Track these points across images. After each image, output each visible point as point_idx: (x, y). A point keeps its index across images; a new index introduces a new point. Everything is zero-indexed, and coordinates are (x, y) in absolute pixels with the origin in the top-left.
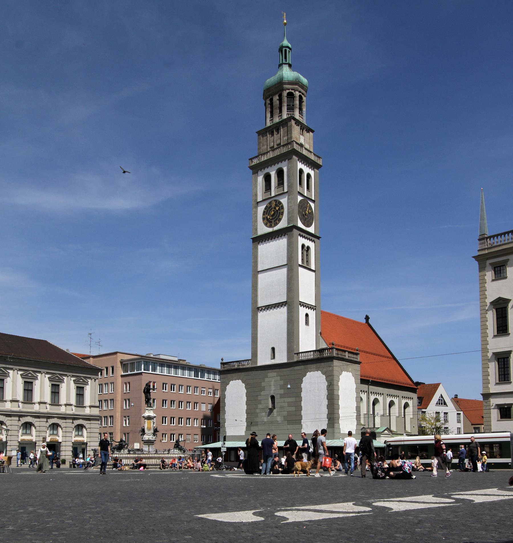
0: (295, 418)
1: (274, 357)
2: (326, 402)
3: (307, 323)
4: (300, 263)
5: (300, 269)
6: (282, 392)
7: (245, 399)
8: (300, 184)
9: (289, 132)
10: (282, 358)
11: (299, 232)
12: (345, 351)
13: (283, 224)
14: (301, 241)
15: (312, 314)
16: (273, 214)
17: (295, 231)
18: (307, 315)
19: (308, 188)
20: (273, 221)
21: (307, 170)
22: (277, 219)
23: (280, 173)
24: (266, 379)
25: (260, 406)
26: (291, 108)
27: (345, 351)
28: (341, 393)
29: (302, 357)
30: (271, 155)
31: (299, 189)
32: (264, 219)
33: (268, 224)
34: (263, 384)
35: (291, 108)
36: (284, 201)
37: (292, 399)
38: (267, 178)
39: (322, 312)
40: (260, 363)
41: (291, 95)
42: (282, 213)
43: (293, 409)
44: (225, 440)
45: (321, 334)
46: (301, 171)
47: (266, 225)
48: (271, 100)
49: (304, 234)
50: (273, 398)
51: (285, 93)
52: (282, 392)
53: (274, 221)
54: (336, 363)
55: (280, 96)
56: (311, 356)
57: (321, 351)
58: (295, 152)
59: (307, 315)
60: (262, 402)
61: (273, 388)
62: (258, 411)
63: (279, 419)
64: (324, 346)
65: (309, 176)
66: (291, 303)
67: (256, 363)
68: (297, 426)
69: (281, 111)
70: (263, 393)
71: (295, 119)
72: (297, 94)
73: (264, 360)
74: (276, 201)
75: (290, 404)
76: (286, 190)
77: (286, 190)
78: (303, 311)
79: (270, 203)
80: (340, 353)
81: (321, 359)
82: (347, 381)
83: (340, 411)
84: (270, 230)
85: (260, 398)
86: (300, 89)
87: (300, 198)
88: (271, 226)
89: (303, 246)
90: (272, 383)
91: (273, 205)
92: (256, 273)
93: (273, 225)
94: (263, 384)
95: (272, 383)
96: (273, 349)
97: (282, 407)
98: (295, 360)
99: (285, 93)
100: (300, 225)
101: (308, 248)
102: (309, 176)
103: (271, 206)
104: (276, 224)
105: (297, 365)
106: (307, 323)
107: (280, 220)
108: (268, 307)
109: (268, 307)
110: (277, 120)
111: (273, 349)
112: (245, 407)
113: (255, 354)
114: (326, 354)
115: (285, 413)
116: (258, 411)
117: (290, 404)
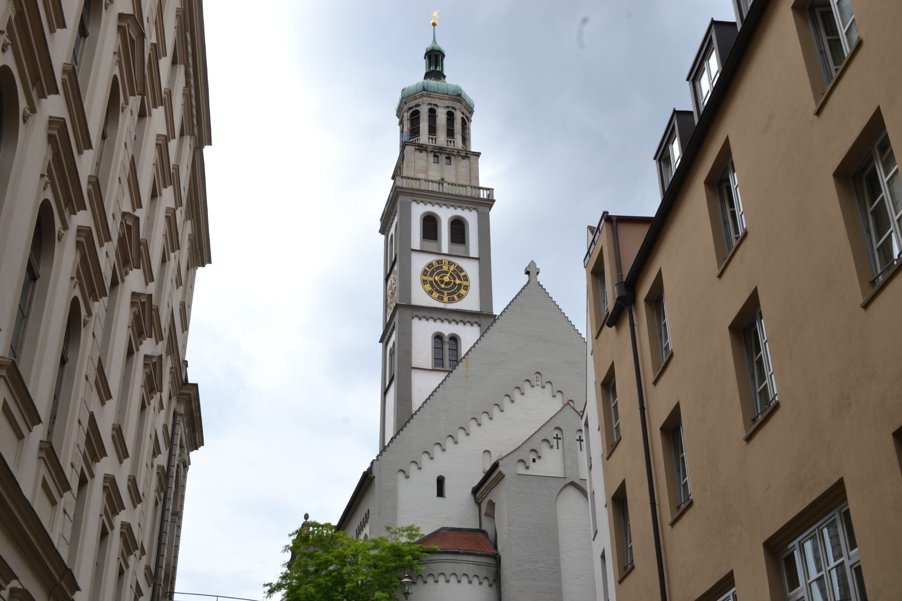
13: (470, 302)
20: (446, 292)
22: (454, 293)
32: (424, 282)
36: (471, 269)
42: (466, 288)
47: (430, 293)
53: (448, 294)
76: (474, 251)
79: (439, 262)
88: (440, 299)
91: (445, 268)
93: (446, 299)
103: (441, 267)
104: (452, 300)
107: (461, 297)
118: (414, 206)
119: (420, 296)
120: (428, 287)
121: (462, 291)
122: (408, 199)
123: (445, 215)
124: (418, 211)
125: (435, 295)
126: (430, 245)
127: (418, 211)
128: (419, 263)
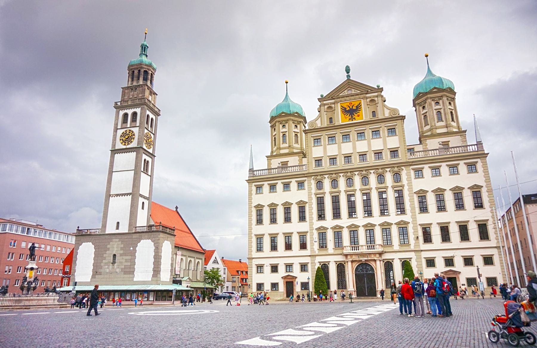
0: (130, 270)
1: (118, 228)
2: (153, 260)
3: (143, 208)
4: (142, 170)
5: (142, 173)
6: (122, 252)
7: (93, 256)
8: (147, 123)
9: (143, 92)
10: (124, 229)
11: (144, 151)
12: (167, 228)
14: (144, 157)
15: (146, 202)
16: (127, 138)
17: (141, 149)
18: (143, 203)
19: (151, 126)
21: (151, 116)
23: (135, 114)
24: (111, 243)
25: (104, 261)
26: (145, 79)
27: (167, 228)
28: (162, 254)
29: (138, 230)
30: (130, 103)
31: (146, 126)
32: (120, 140)
33: (123, 143)
34: (108, 246)
35: (145, 79)
36: (136, 130)
37: (129, 257)
38: (126, 115)
39: (153, 202)
40: (107, 233)
41: (146, 72)
43: (129, 264)
44: (75, 284)
45: (150, 216)
46: (148, 116)
48: (133, 72)
49: (146, 153)
50: (115, 255)
51: (142, 70)
52: (122, 252)
54: (162, 235)
55: (139, 71)
56: (145, 229)
57: (150, 226)
58: (145, 104)
59: (143, 203)
60: (107, 258)
61: (115, 249)
62: (102, 264)
63: (118, 270)
64: (152, 223)
65: (152, 119)
66: (135, 194)
67: (105, 231)
68: (131, 276)
69: (139, 79)
70: (107, 252)
71: (147, 86)
72: (150, 72)
73: (111, 229)
74: (130, 130)
75: (126, 261)
76: (138, 124)
77: (138, 125)
78: (141, 200)
79: (126, 131)
80: (164, 228)
81: (150, 231)
82: (167, 247)
83: (162, 266)
84: (124, 147)
85: (105, 255)
86: (152, 70)
87: (146, 131)
88: (125, 145)
89: (145, 160)
90: (115, 246)
91: (128, 133)
92: (111, 172)
94: (108, 246)
95: (115, 246)
96: (118, 223)
97: (121, 263)
98: (134, 231)
99: (142, 70)
100: (144, 147)
101: (148, 161)
102: (152, 119)
104: (128, 144)
105: (134, 235)
106: (143, 208)
108: (117, 195)
109: (117, 195)
110: (135, 83)
111: (118, 223)
112: (93, 262)
113: (104, 226)
114: (154, 229)
115: (123, 267)
116: (102, 264)
117: (126, 261)
118: (120, 111)
119: (120, 145)
120: (121, 141)
121: (132, 140)
122: (118, 110)
123: (130, 112)
124: (122, 113)
125: (123, 143)
126: (124, 125)
127: (122, 113)
128: (120, 132)
